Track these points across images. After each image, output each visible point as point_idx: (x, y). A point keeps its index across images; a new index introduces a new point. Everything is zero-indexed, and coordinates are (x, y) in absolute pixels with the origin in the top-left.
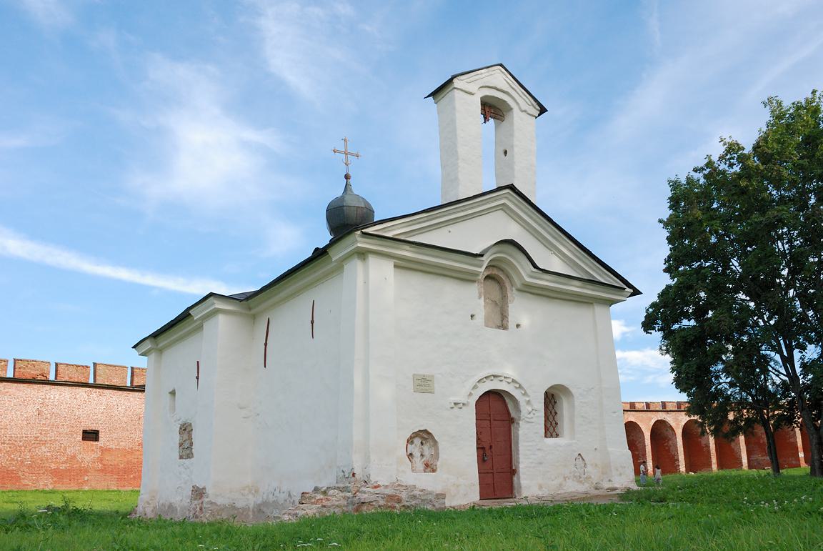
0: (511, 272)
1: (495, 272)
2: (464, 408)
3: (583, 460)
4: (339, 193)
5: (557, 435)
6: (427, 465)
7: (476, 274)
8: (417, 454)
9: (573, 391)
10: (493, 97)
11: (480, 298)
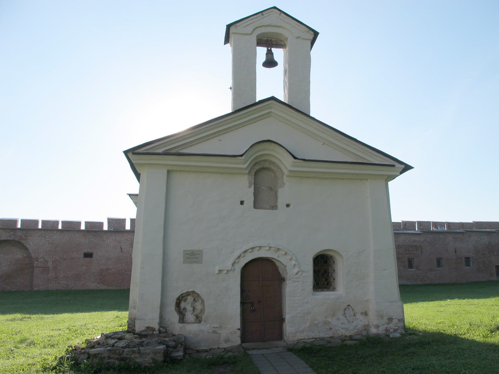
3: (353, 310)
6: (197, 317)
8: (189, 308)
10: (269, 33)
11: (250, 187)
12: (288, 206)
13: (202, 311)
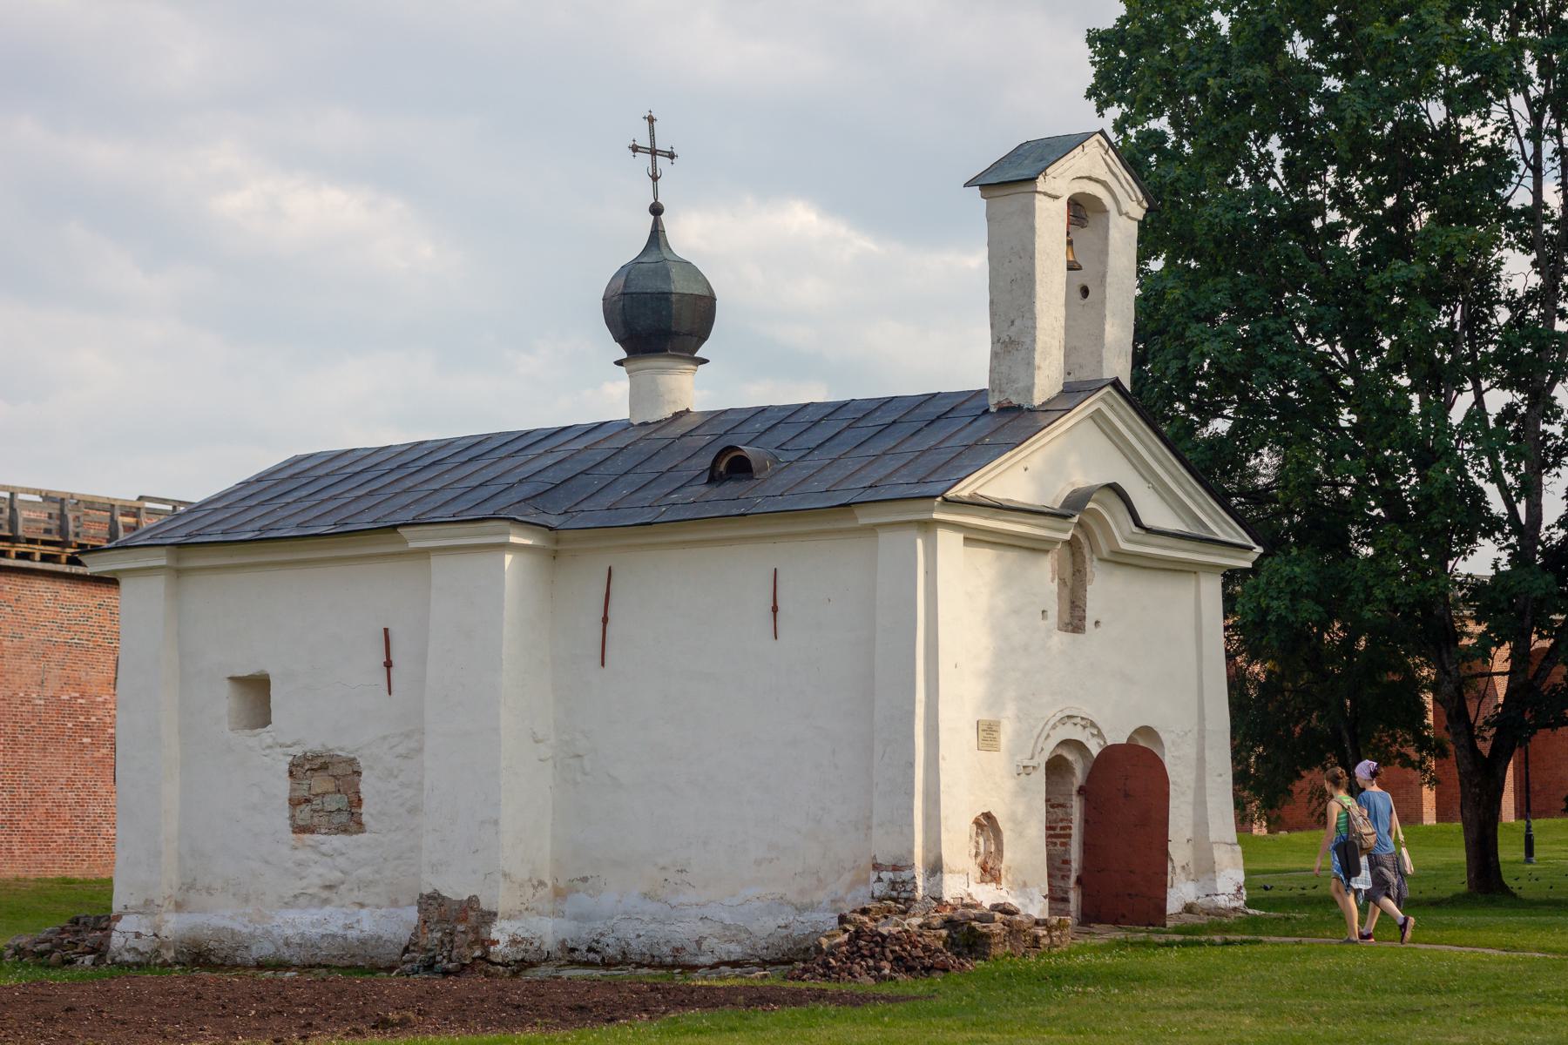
4: (632, 246)
10: (1083, 194)
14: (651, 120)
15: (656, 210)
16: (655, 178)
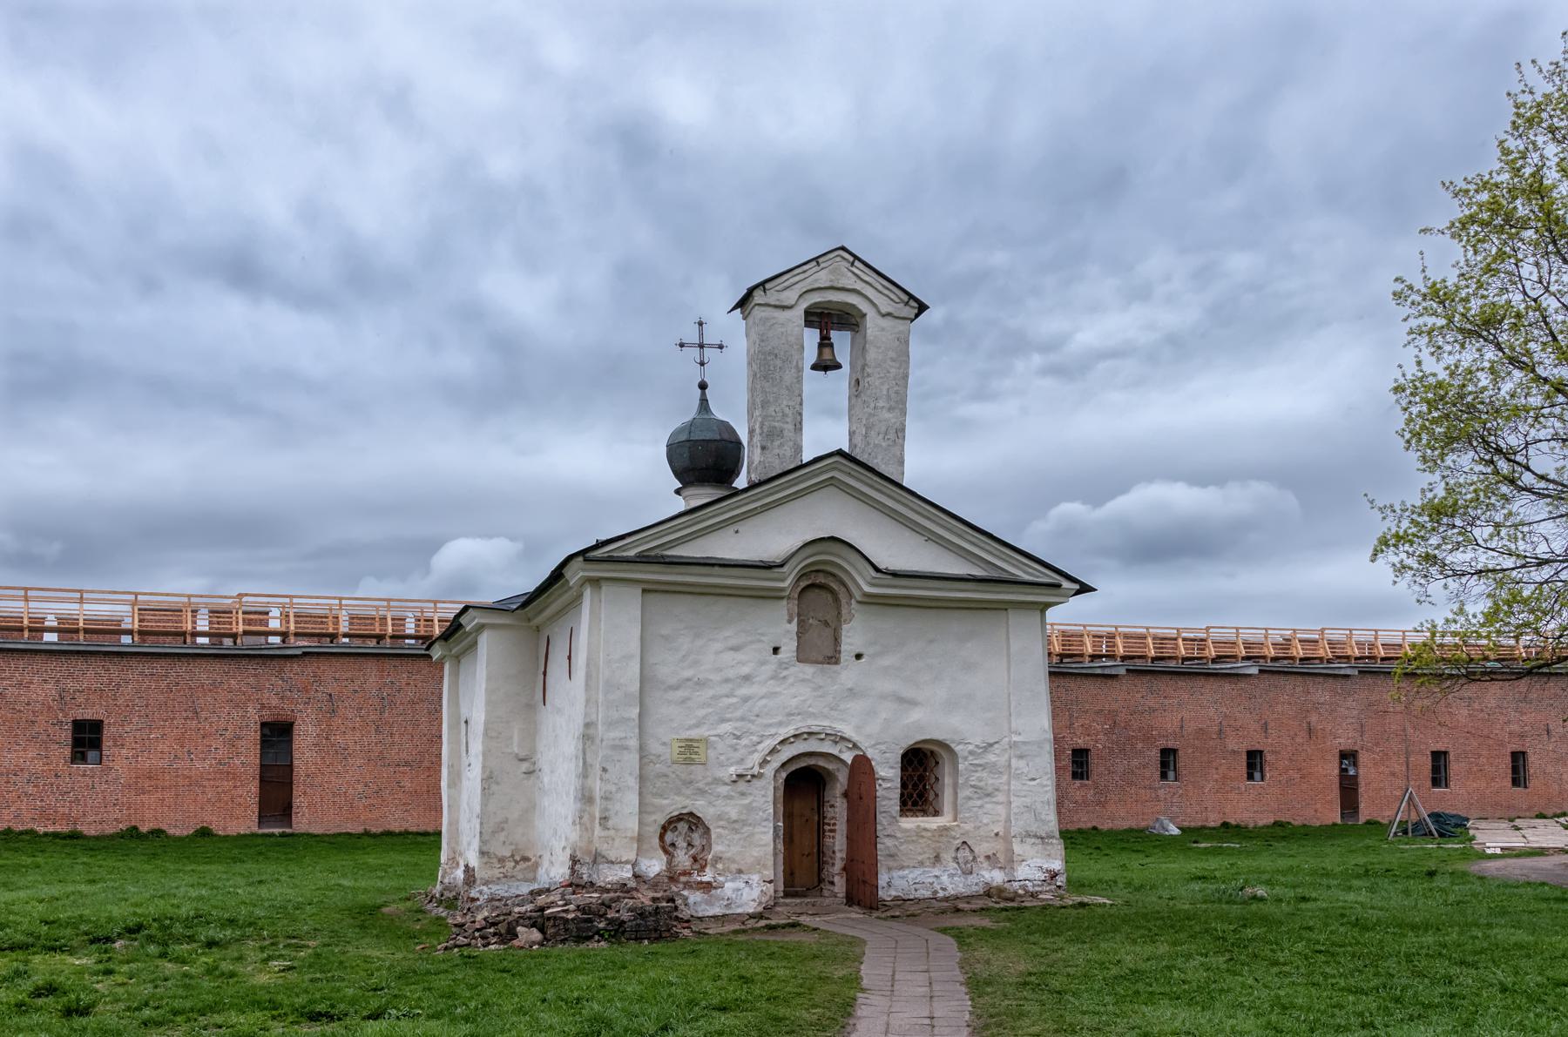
0: (834, 586)
1: (821, 579)
2: (755, 781)
4: (690, 413)
5: (937, 813)
6: (695, 859)
7: (782, 589)
8: (681, 843)
9: (957, 749)
11: (790, 622)
12: (859, 656)
13: (706, 848)
14: (701, 324)
15: (703, 386)
16: (702, 364)
